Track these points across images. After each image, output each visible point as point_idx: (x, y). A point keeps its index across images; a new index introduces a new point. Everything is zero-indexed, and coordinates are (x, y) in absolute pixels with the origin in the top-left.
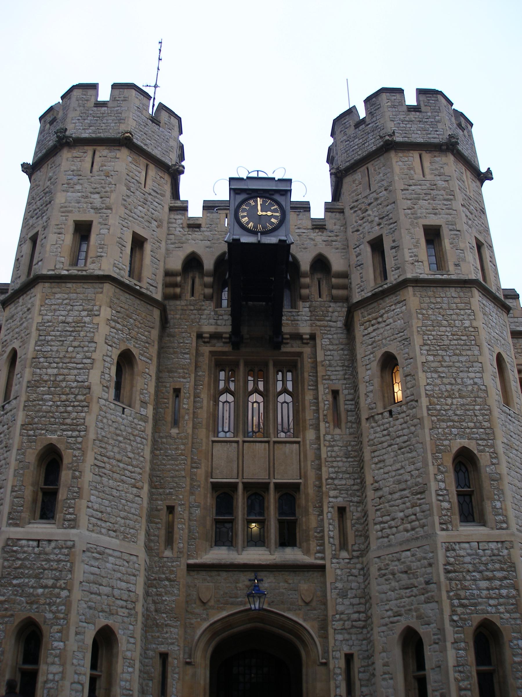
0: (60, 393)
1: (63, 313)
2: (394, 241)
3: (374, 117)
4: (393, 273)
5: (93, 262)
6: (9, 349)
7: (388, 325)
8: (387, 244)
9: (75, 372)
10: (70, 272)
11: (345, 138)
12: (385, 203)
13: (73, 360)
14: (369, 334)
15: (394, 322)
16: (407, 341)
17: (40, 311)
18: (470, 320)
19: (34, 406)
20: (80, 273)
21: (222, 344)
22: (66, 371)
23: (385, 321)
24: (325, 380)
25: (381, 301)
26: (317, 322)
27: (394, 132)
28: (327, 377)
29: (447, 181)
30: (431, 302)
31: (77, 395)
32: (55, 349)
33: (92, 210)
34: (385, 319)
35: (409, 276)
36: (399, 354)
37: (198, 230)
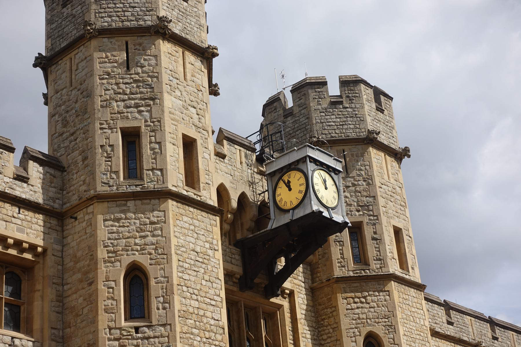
0: (204, 328)
1: (193, 240)
2: (375, 233)
3: (352, 103)
4: (376, 262)
5: (204, 189)
6: (127, 260)
7: (372, 308)
8: (368, 232)
9: (211, 308)
10: (189, 193)
11: (320, 107)
12: (365, 194)
13: (208, 295)
14: (352, 309)
15: (378, 307)
16: (392, 328)
17: (175, 232)
18: (423, 319)
19: (187, 338)
20: (195, 197)
21: (231, 283)
22: (204, 306)
23: (369, 303)
24: (303, 337)
25: (364, 284)
26: (294, 279)
27: (379, 132)
28: (304, 335)
29: (400, 187)
30: (403, 298)
31: (216, 333)
32: (193, 279)
33: (193, 127)
34: (368, 301)
35: (391, 271)
36: (385, 337)
37: (222, 160)
